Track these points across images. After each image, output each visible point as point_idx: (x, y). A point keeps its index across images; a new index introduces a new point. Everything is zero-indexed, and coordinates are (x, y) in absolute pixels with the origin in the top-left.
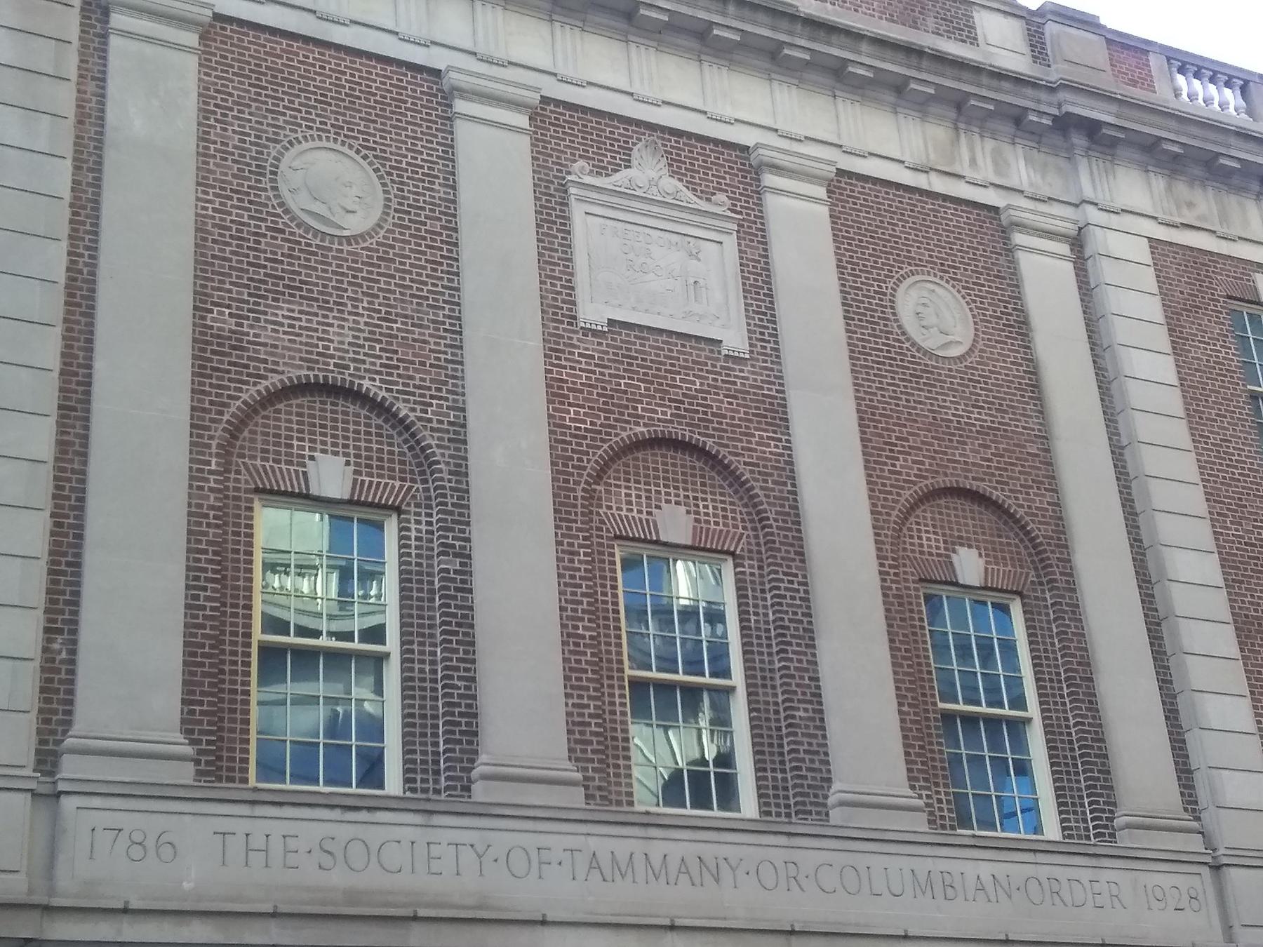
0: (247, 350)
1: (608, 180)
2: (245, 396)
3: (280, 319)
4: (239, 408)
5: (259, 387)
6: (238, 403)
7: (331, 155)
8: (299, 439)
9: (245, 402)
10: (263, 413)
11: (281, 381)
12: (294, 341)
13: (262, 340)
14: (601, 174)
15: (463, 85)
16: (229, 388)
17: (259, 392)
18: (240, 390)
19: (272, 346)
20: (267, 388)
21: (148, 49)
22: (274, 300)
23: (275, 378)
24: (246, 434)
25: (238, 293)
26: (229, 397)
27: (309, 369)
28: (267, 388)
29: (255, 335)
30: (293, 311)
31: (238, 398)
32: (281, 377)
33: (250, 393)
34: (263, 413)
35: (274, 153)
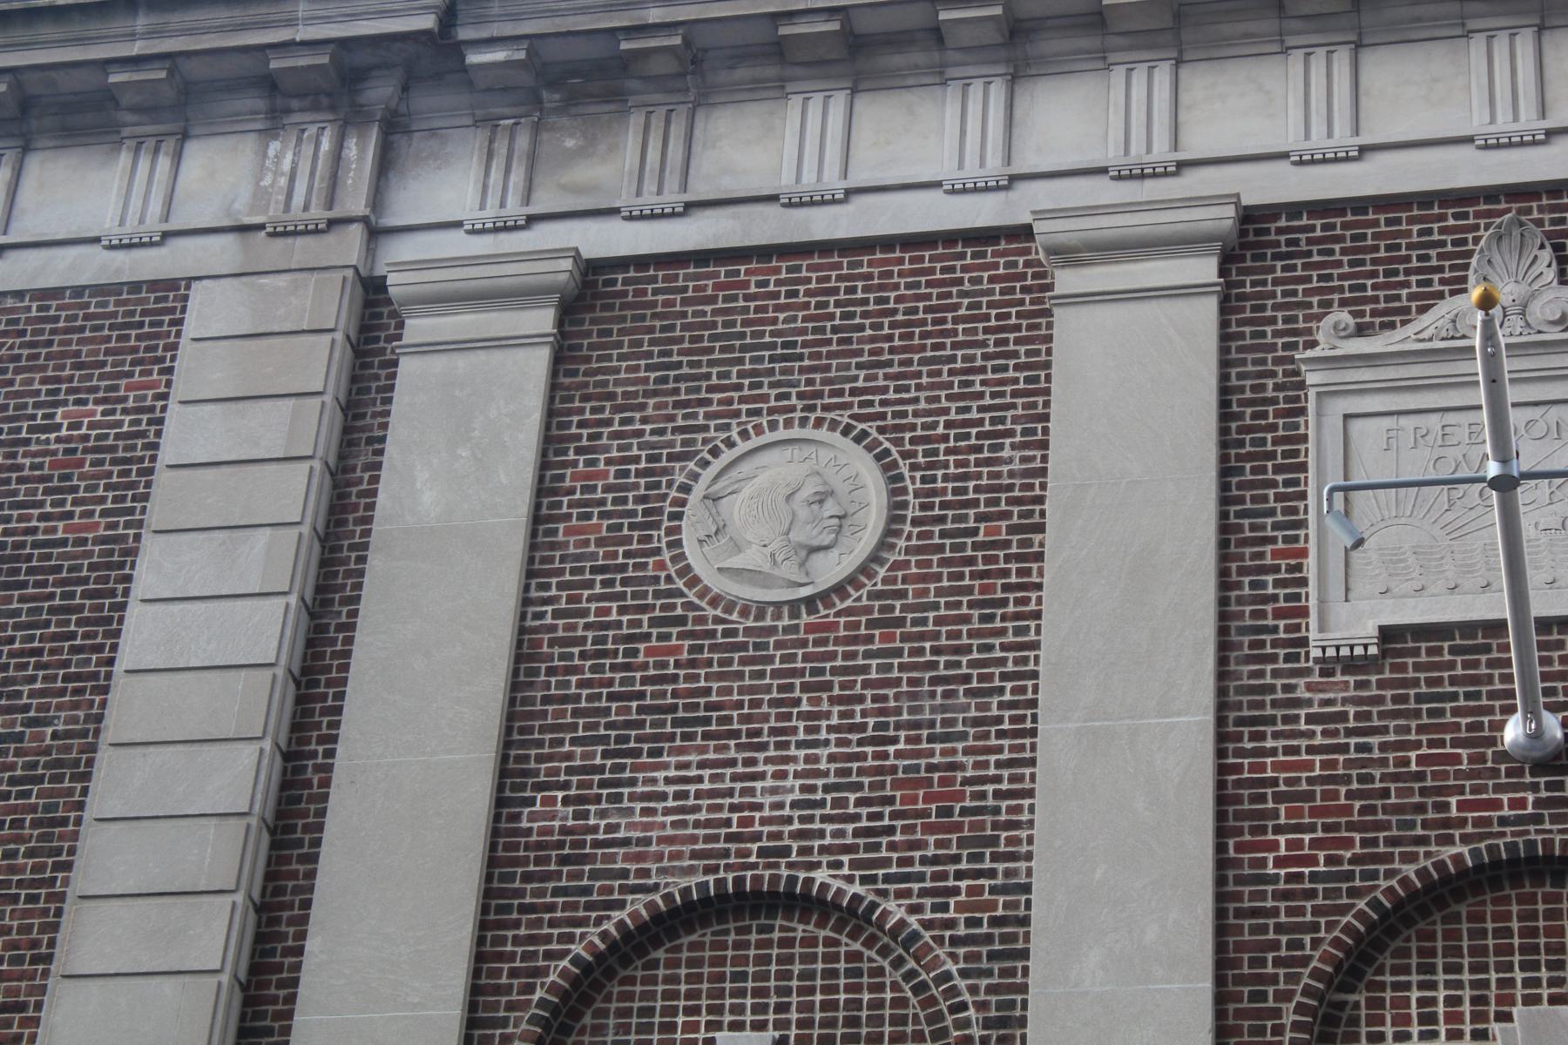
0: (590, 859)
1: (1400, 333)
2: (577, 948)
3: (661, 787)
4: (564, 974)
5: (606, 926)
6: (565, 963)
7: (788, 452)
8: (689, 1011)
9: (576, 961)
10: (623, 973)
11: (650, 906)
12: (684, 824)
13: (621, 835)
14: (1392, 325)
15: (1061, 239)
16: (548, 939)
17: (604, 935)
18: (570, 938)
19: (639, 842)
20: (621, 925)
21: (461, 362)
22: (651, 753)
23: (638, 904)
24: (588, 1020)
25: (585, 756)
26: (549, 955)
27: (708, 870)
28: (621, 925)
29: (611, 828)
30: (686, 766)
31: (562, 955)
32: (649, 897)
33: (588, 940)
34: (623, 973)
35: (680, 479)
